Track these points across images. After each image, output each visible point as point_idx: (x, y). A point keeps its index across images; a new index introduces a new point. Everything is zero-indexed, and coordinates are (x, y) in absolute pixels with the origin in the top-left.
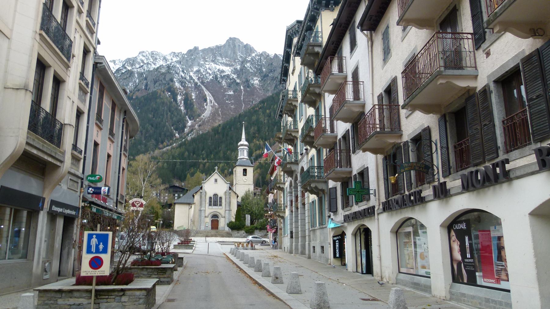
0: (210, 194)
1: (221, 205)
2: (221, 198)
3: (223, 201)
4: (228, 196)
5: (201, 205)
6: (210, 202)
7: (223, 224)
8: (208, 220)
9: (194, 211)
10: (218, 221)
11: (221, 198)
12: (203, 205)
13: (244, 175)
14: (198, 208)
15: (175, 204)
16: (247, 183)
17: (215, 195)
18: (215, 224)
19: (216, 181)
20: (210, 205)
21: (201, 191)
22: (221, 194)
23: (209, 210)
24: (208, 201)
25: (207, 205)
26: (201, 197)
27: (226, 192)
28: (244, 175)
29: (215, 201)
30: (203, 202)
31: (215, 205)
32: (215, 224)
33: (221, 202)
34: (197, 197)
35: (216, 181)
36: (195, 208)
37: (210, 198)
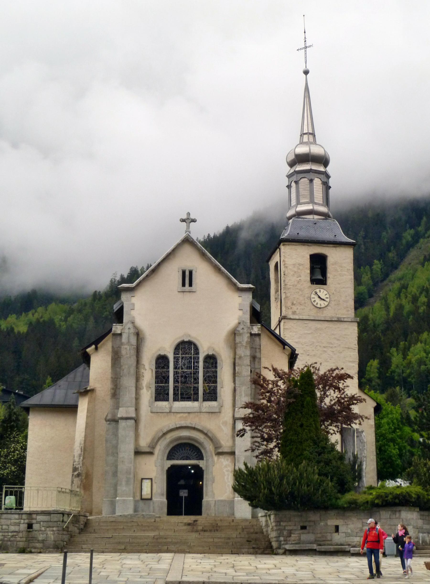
0: (161, 341)
1: (212, 395)
2: (212, 360)
3: (225, 374)
4: (244, 352)
5: (115, 393)
6: (161, 378)
7: (220, 485)
8: (154, 472)
9: (90, 427)
10: (199, 474)
11: (212, 360)
12: (128, 396)
13: (314, 281)
14: (105, 408)
15: (27, 410)
16: (328, 314)
17: (186, 348)
18: (184, 490)
19: (187, 278)
20: (161, 395)
21: (117, 328)
22: (211, 340)
23: (161, 419)
24: (148, 376)
25: (147, 395)
26: (116, 358)
27: (234, 333)
28: (314, 281)
29: (186, 374)
30: (128, 382)
31: (186, 394)
32: (184, 490)
33: (212, 378)
34: (100, 364)
35: (187, 278)
36: (91, 413)
37: (161, 361)
